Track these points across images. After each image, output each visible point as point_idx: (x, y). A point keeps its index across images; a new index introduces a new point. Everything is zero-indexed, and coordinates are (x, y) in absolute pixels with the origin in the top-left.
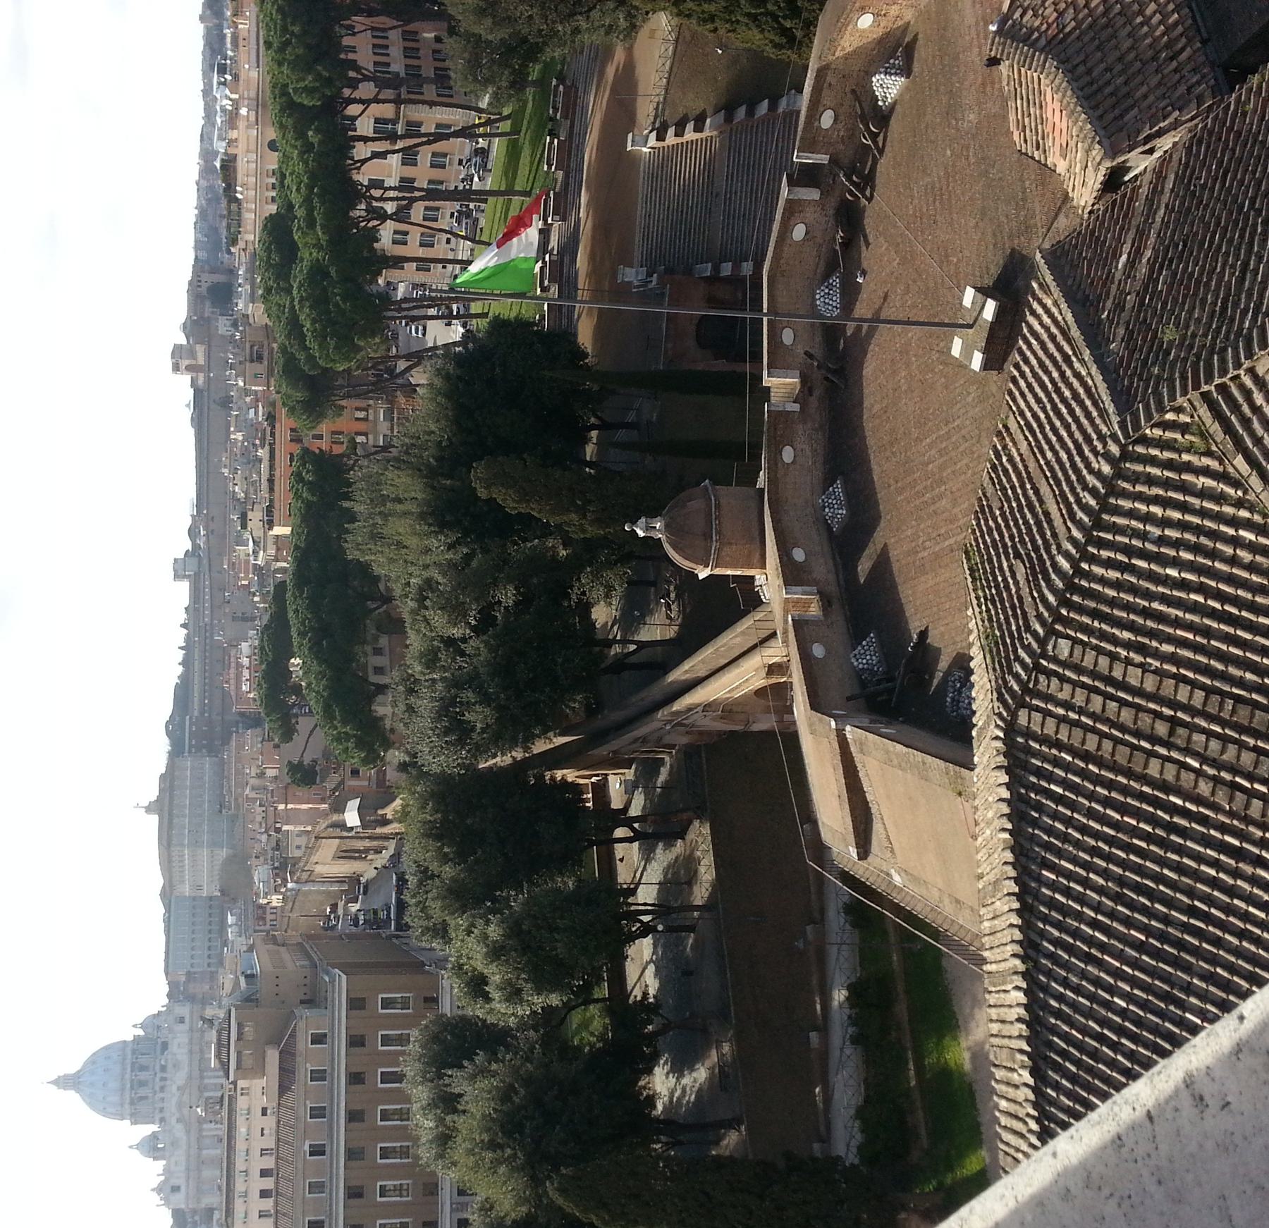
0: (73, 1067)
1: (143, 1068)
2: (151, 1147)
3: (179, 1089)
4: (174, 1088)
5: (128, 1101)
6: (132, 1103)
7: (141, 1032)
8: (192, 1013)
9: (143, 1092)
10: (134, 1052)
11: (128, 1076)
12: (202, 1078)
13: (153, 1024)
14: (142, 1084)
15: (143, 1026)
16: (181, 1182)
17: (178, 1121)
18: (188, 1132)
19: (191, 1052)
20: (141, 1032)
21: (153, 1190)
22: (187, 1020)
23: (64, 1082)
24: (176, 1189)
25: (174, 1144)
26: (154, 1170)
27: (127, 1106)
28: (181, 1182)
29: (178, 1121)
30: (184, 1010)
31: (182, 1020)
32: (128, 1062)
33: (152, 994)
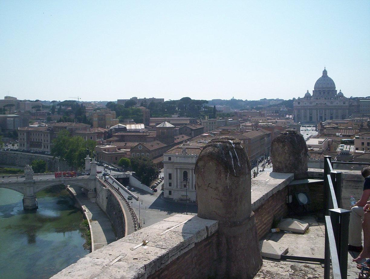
0: (329, 75)
1: (328, 93)
2: (307, 96)
3: (325, 103)
4: (326, 102)
5: (320, 90)
6: (319, 91)
7: (338, 92)
8: (346, 106)
9: (322, 93)
10: (333, 90)
11: (326, 89)
12: (328, 109)
13: (341, 95)
14: (324, 93)
15: (340, 93)
16: (301, 105)
17: (317, 103)
18: (314, 106)
19: (335, 106)
20: (338, 92)
21: (299, 97)
22: (344, 105)
23: (325, 72)
24: (299, 103)
25: (311, 103)
26: (302, 96)
27: (318, 89)
28: (301, 105)
29: (317, 103)
30: (347, 104)
31: (344, 103)
32: (330, 89)
33: (347, 95)
